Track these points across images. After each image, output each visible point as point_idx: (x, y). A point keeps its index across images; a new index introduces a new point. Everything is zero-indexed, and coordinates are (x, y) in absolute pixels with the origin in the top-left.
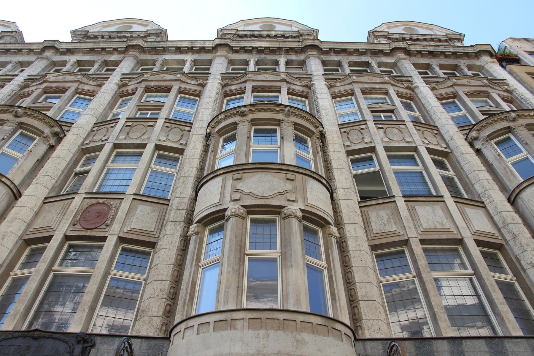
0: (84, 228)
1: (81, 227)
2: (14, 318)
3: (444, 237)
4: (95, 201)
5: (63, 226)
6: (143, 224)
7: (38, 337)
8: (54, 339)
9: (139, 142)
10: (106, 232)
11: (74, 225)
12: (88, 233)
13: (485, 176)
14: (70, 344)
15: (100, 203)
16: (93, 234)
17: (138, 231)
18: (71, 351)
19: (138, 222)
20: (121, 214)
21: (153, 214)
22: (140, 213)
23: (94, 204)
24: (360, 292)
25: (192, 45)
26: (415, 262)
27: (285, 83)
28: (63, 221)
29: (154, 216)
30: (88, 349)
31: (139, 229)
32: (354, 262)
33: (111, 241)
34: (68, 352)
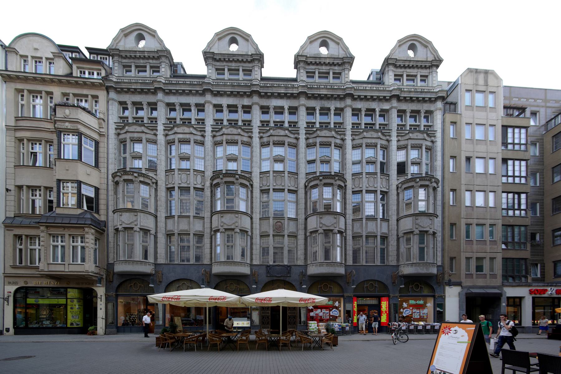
3: (372, 235)
4: (277, 221)
9: (281, 187)
12: (279, 234)
13: (395, 208)
16: (280, 234)
20: (286, 226)
24: (348, 253)
25: (286, 90)
26: (362, 243)
27: (333, 138)
32: (348, 244)
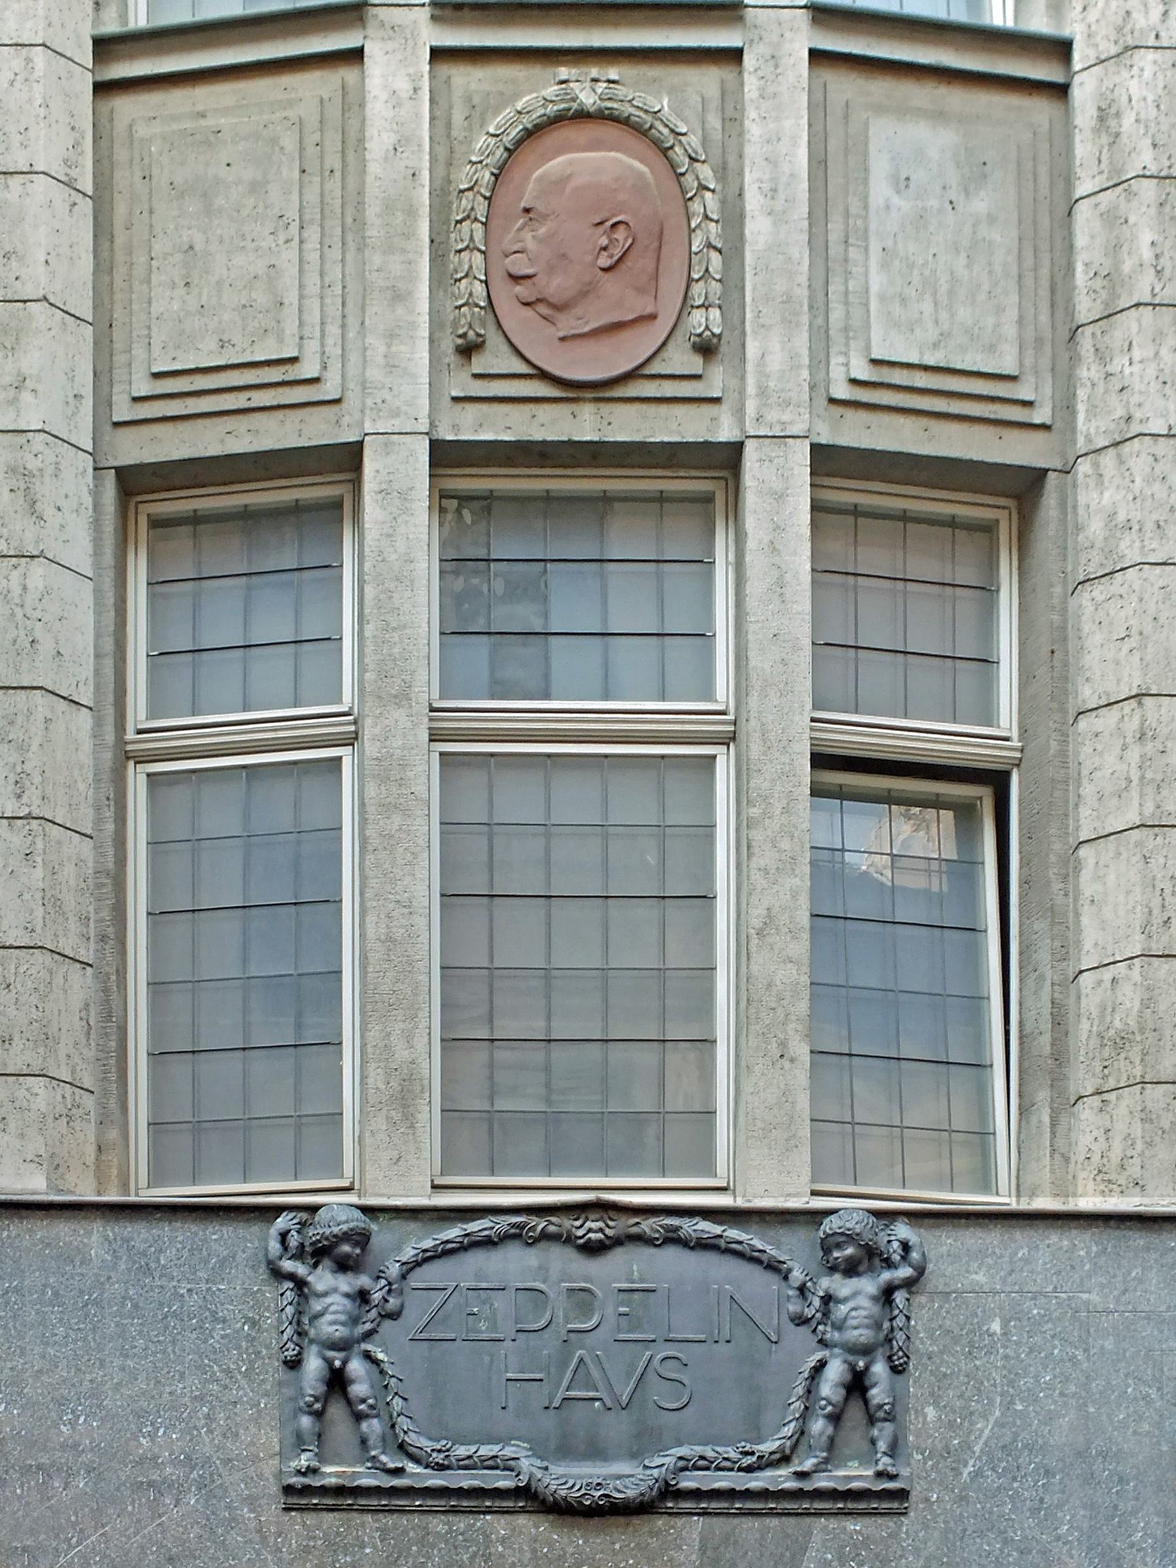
0: (543, 375)
1: (523, 369)
2: (409, 1120)
5: (391, 366)
6: (944, 315)
7: (607, 1242)
8: (692, 1248)
10: (707, 410)
11: (468, 350)
14: (797, 1276)
15: (583, 116)
17: (921, 380)
18: (819, 1315)
19: (904, 301)
21: (980, 205)
22: (896, 200)
23: (530, 134)
28: (377, 309)
29: (991, 219)
30: (899, 1297)
31: (926, 368)
33: (780, 497)
34: (800, 1321)
